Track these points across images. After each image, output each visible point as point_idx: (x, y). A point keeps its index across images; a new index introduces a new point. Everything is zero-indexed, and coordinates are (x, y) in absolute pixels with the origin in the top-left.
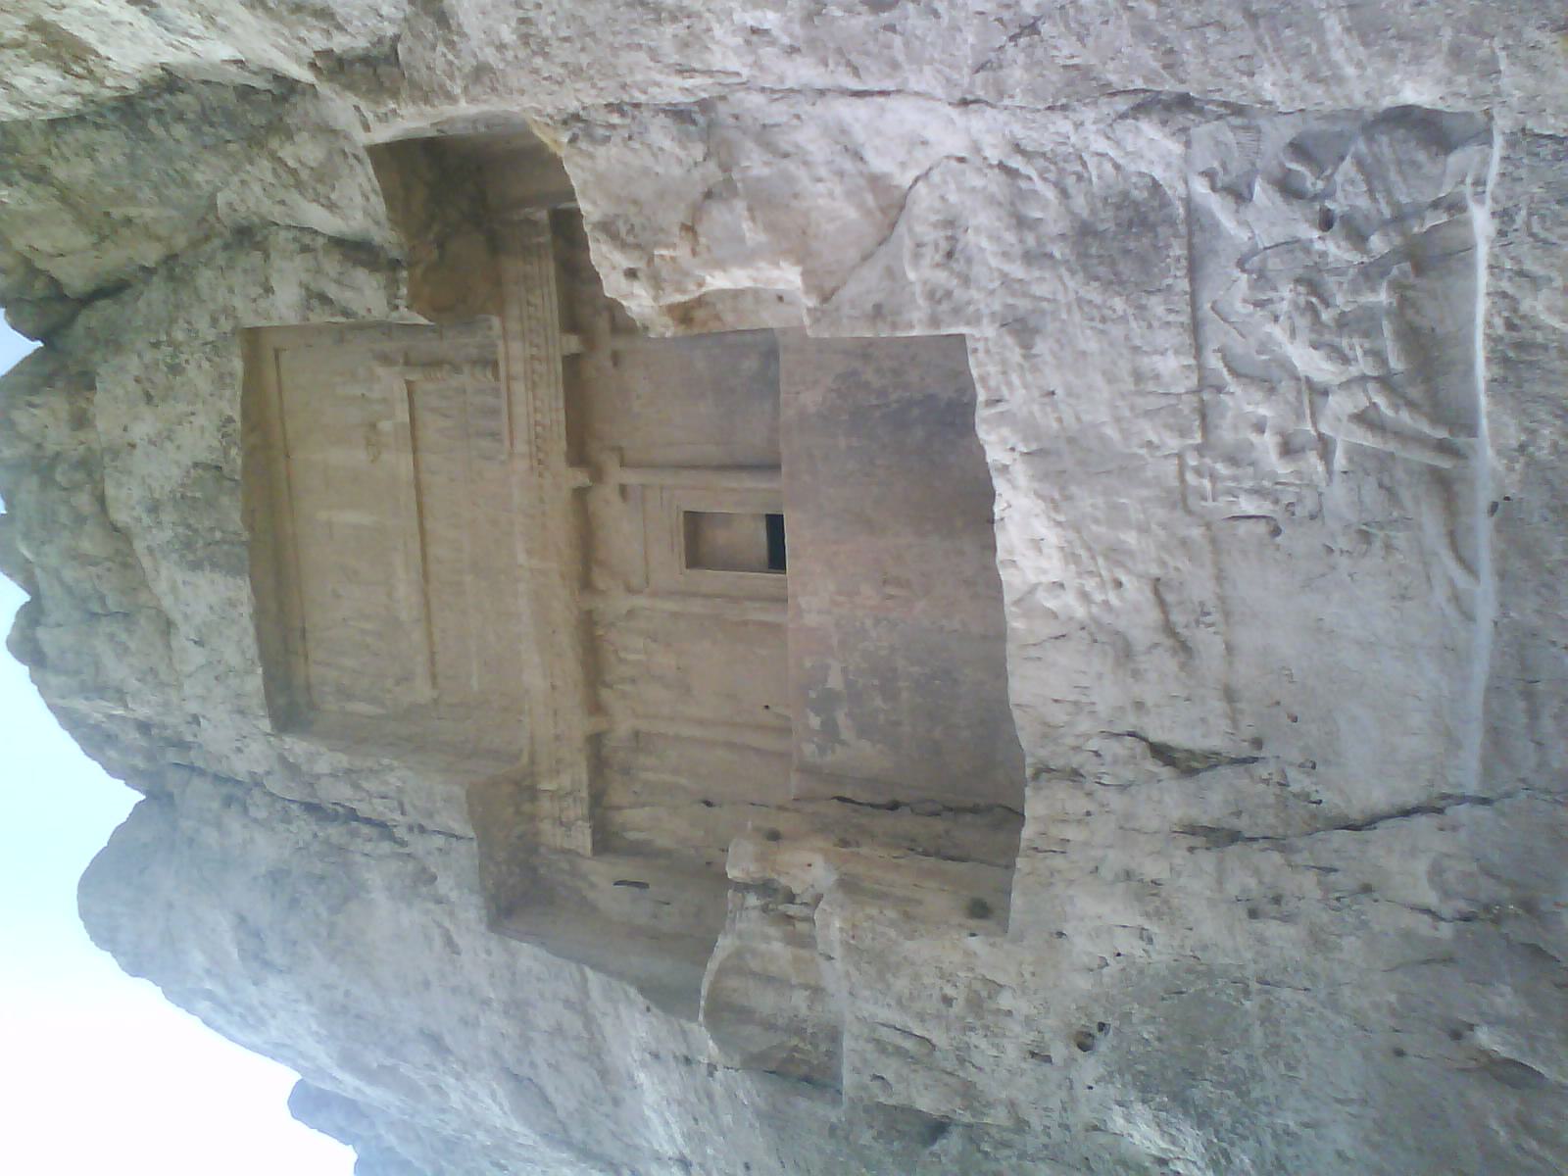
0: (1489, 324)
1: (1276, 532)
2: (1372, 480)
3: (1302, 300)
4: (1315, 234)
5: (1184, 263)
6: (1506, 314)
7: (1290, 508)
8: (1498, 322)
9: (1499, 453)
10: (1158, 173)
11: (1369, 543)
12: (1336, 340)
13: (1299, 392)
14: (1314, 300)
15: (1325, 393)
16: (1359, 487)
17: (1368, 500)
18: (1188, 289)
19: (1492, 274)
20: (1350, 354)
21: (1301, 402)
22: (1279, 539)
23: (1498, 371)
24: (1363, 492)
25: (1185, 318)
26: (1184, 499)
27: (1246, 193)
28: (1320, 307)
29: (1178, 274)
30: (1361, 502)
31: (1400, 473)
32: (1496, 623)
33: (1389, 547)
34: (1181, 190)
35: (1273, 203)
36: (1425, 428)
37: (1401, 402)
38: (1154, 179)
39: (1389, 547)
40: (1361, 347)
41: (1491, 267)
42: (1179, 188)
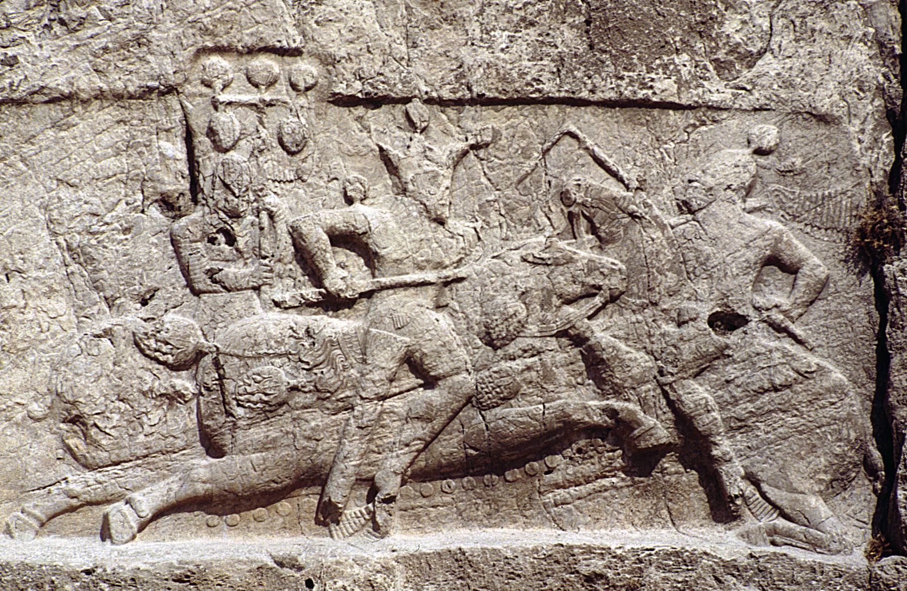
0: (589, 550)
1: (167, 204)
2: (302, 379)
3: (599, 281)
4: (705, 310)
5: (641, 94)
6: (610, 574)
7: (221, 238)
8: (597, 565)
9: (387, 570)
10: (769, 65)
11: (175, 368)
12: (533, 329)
13: (440, 266)
14: (598, 301)
15: (438, 307)
16: (287, 354)
17: (264, 367)
18: (598, 96)
19: (668, 555)
20: (512, 349)
21: (421, 268)
22: (154, 211)
23: (526, 565)
24: (278, 361)
25: (549, 87)
26: (220, 50)
27: (752, 202)
28: (587, 306)
29: (623, 83)
30: (259, 357)
31: (317, 419)
32: (88, 572)
33: (174, 398)
34: (746, 102)
35: (747, 246)
36: (397, 461)
37: (437, 424)
38: (760, 54)
39: (174, 398)
40: (529, 368)
41: (677, 554)
42: (751, 97)
